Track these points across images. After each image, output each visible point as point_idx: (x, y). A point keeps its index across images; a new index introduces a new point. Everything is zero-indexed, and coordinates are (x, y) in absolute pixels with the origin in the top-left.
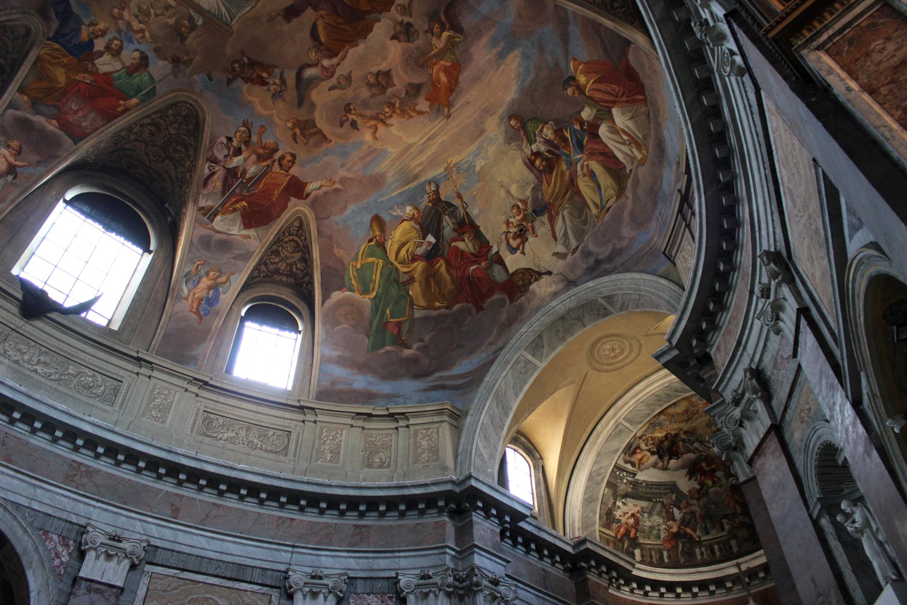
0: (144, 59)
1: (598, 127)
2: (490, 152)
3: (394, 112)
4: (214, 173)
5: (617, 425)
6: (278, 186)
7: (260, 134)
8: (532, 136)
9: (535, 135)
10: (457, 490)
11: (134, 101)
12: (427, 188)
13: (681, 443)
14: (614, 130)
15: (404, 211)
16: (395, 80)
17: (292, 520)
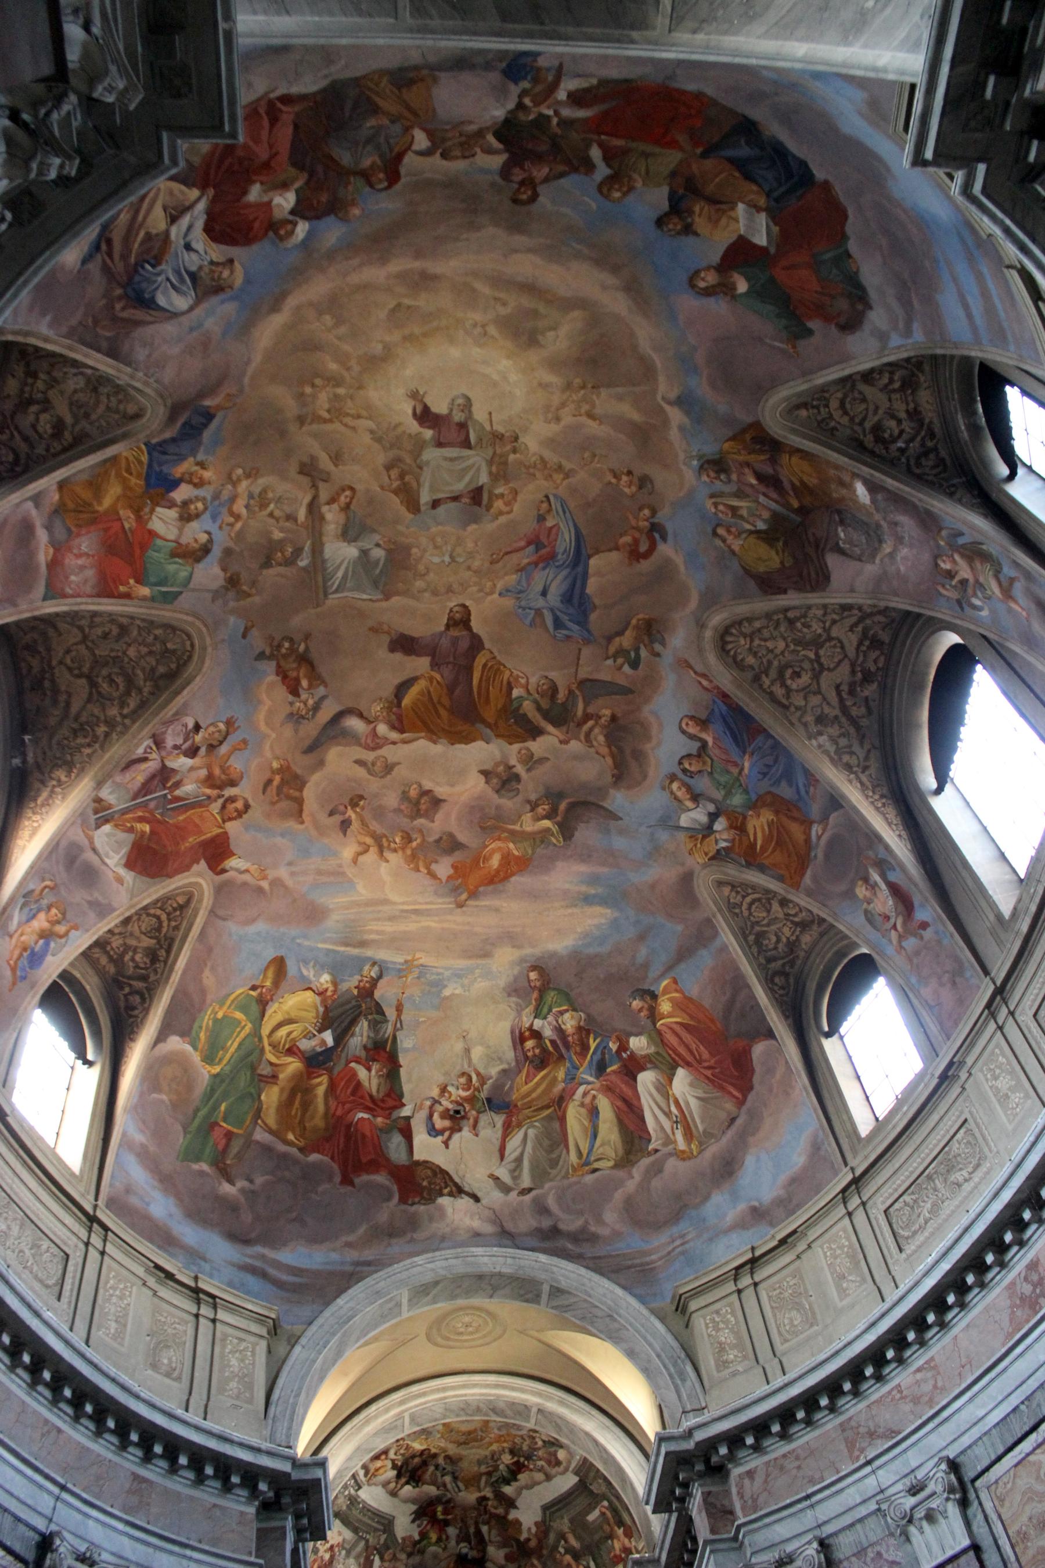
0: (206, 549)
1: (643, 1069)
2: (477, 986)
3: (403, 849)
4: (145, 759)
5: (400, 1416)
6: (200, 832)
7: (235, 749)
8: (545, 1010)
9: (550, 1010)
10: (296, 1475)
11: (145, 591)
12: (367, 968)
13: (432, 1468)
14: (664, 1089)
15: (318, 975)
16: (439, 816)
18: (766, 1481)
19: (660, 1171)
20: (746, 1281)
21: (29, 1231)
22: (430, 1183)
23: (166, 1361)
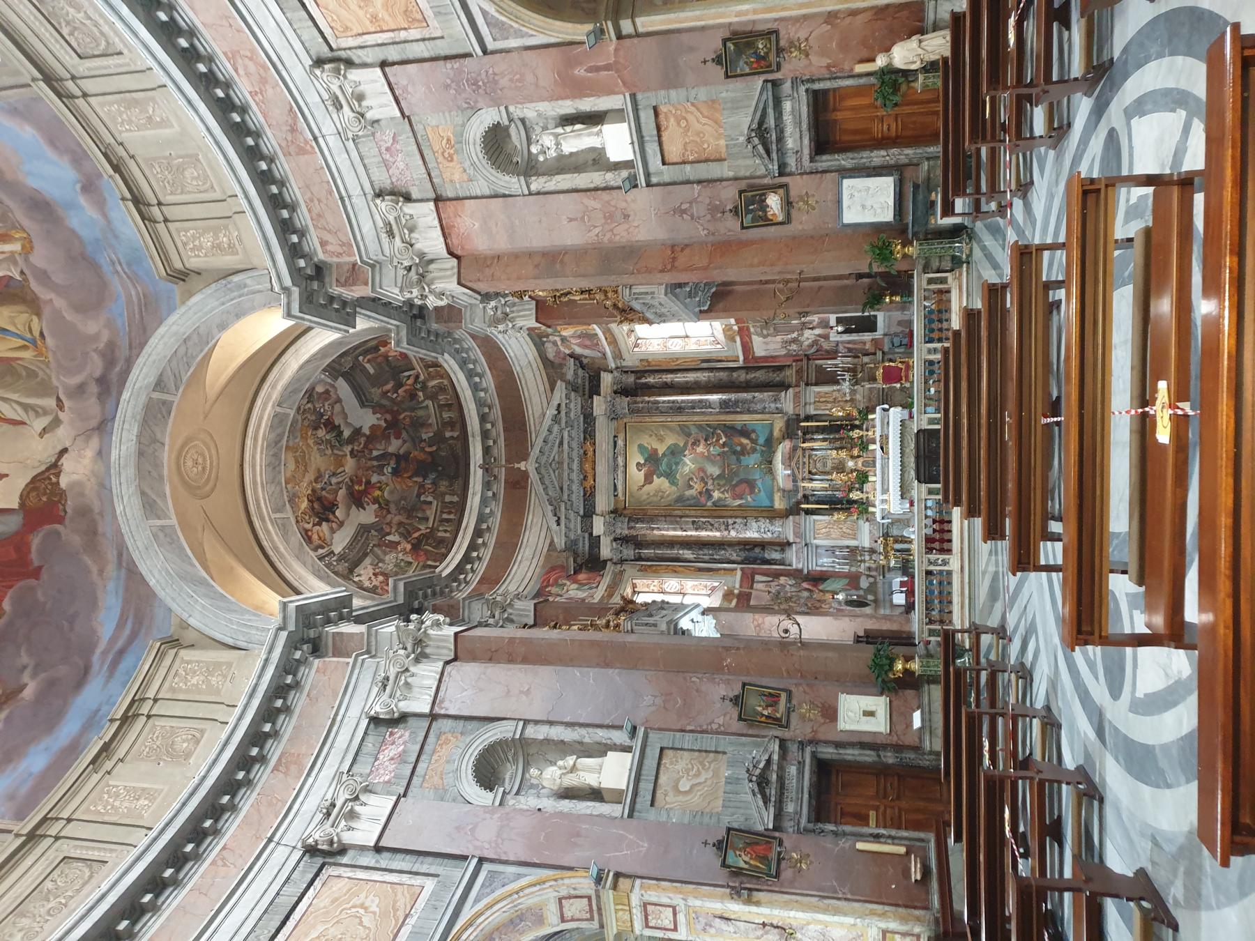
10: (292, 627)
17: (224, 848)
18: (329, 231)
19: (45, 272)
20: (155, 211)
21: (29, 906)
22: (45, 494)
23: (185, 745)
